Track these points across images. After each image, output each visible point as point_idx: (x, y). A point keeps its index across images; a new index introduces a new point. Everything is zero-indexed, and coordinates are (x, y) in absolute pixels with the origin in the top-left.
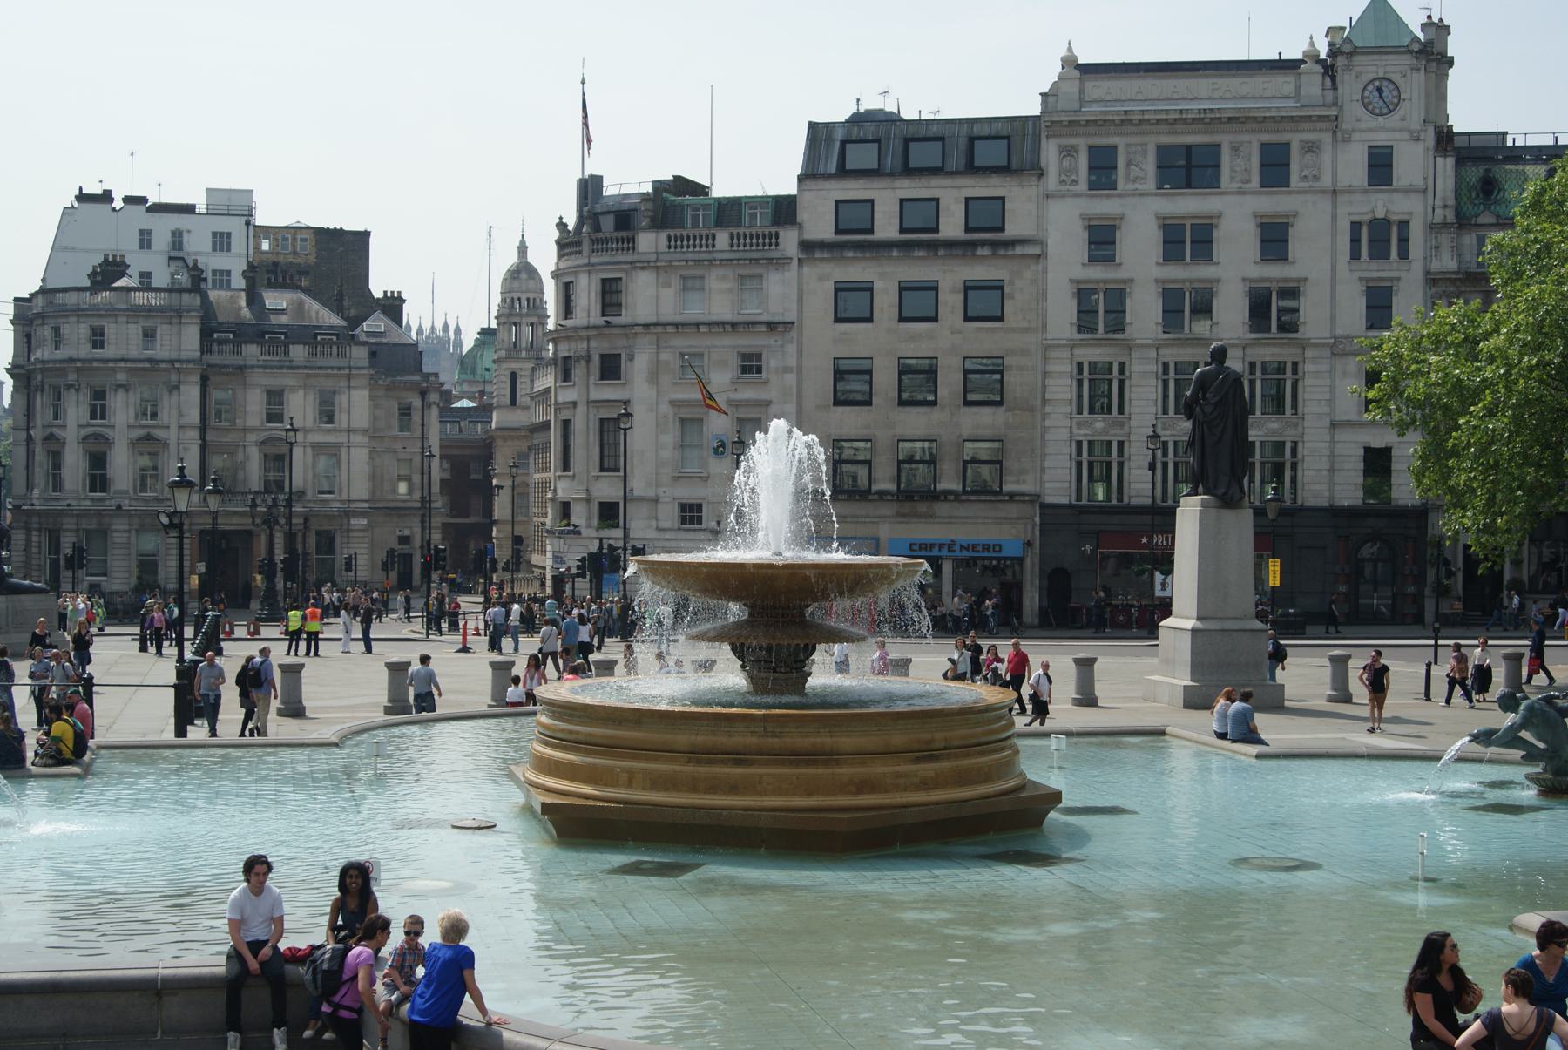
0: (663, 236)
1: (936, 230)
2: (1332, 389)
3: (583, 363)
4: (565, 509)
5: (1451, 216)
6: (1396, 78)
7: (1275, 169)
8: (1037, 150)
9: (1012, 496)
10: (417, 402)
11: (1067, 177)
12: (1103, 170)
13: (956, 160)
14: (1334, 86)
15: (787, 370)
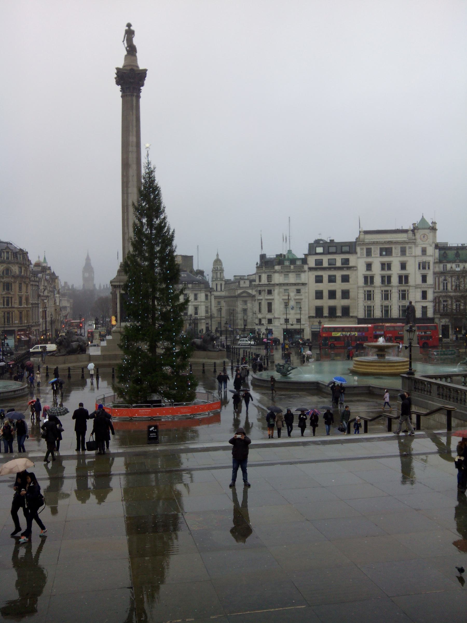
0: (280, 266)
1: (335, 265)
2: (415, 295)
3: (264, 291)
4: (260, 320)
5: (438, 260)
6: (427, 234)
7: (403, 252)
8: (355, 249)
9: (352, 317)
10: (209, 294)
11: (362, 254)
12: (369, 253)
13: (339, 251)
14: (415, 236)
15: (306, 293)
